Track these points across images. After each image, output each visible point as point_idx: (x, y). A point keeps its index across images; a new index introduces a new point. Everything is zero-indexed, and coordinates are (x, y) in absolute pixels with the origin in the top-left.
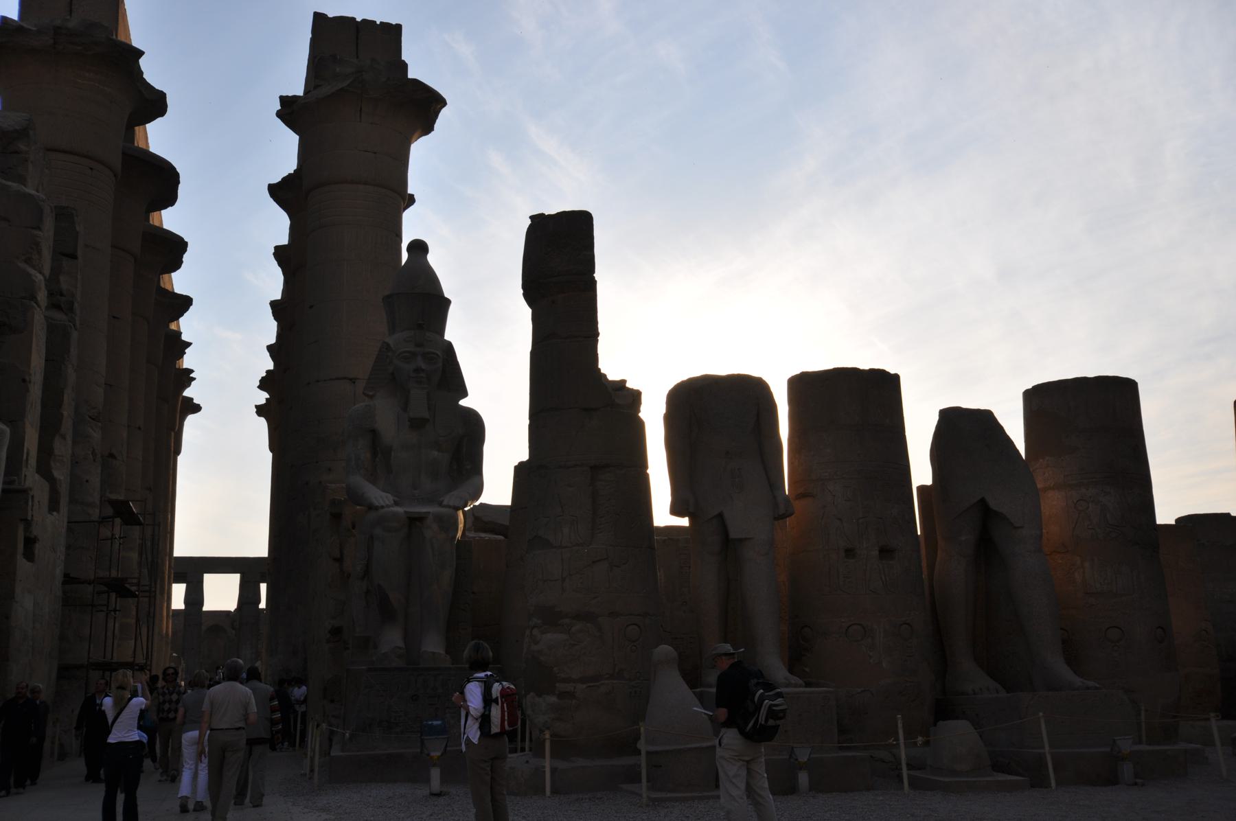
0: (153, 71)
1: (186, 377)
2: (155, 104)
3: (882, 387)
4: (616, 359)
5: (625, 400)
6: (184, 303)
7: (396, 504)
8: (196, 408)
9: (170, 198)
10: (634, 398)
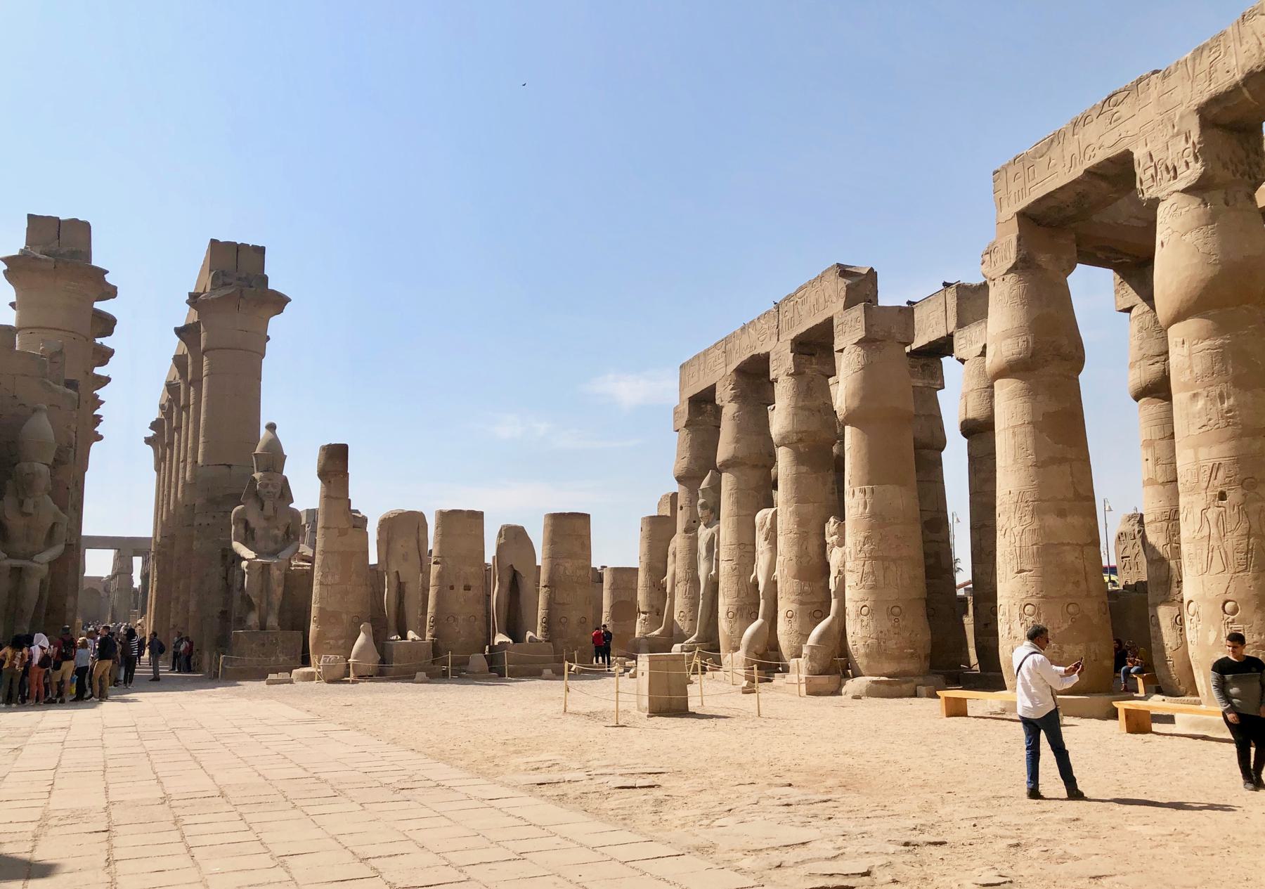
0: (109, 278)
1: (98, 420)
2: (110, 292)
3: (476, 518)
6: (107, 380)
8: (101, 438)
9: (108, 332)
10: (364, 520)
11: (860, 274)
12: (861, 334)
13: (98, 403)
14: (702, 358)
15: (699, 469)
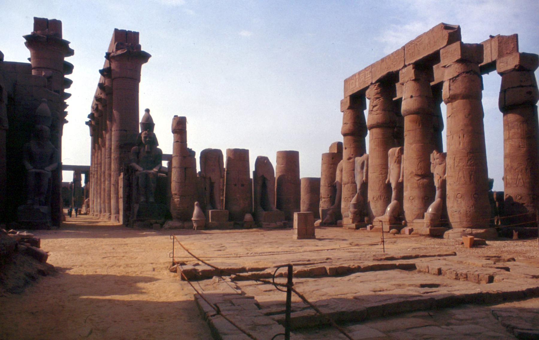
0: (71, 46)
1: (66, 114)
2: (71, 53)
4: (191, 144)
5: (192, 153)
6: (69, 95)
7: (144, 170)
8: (67, 122)
10: (193, 153)
11: (455, 28)
12: (458, 56)
13: (65, 106)
14: (357, 77)
15: (356, 130)
